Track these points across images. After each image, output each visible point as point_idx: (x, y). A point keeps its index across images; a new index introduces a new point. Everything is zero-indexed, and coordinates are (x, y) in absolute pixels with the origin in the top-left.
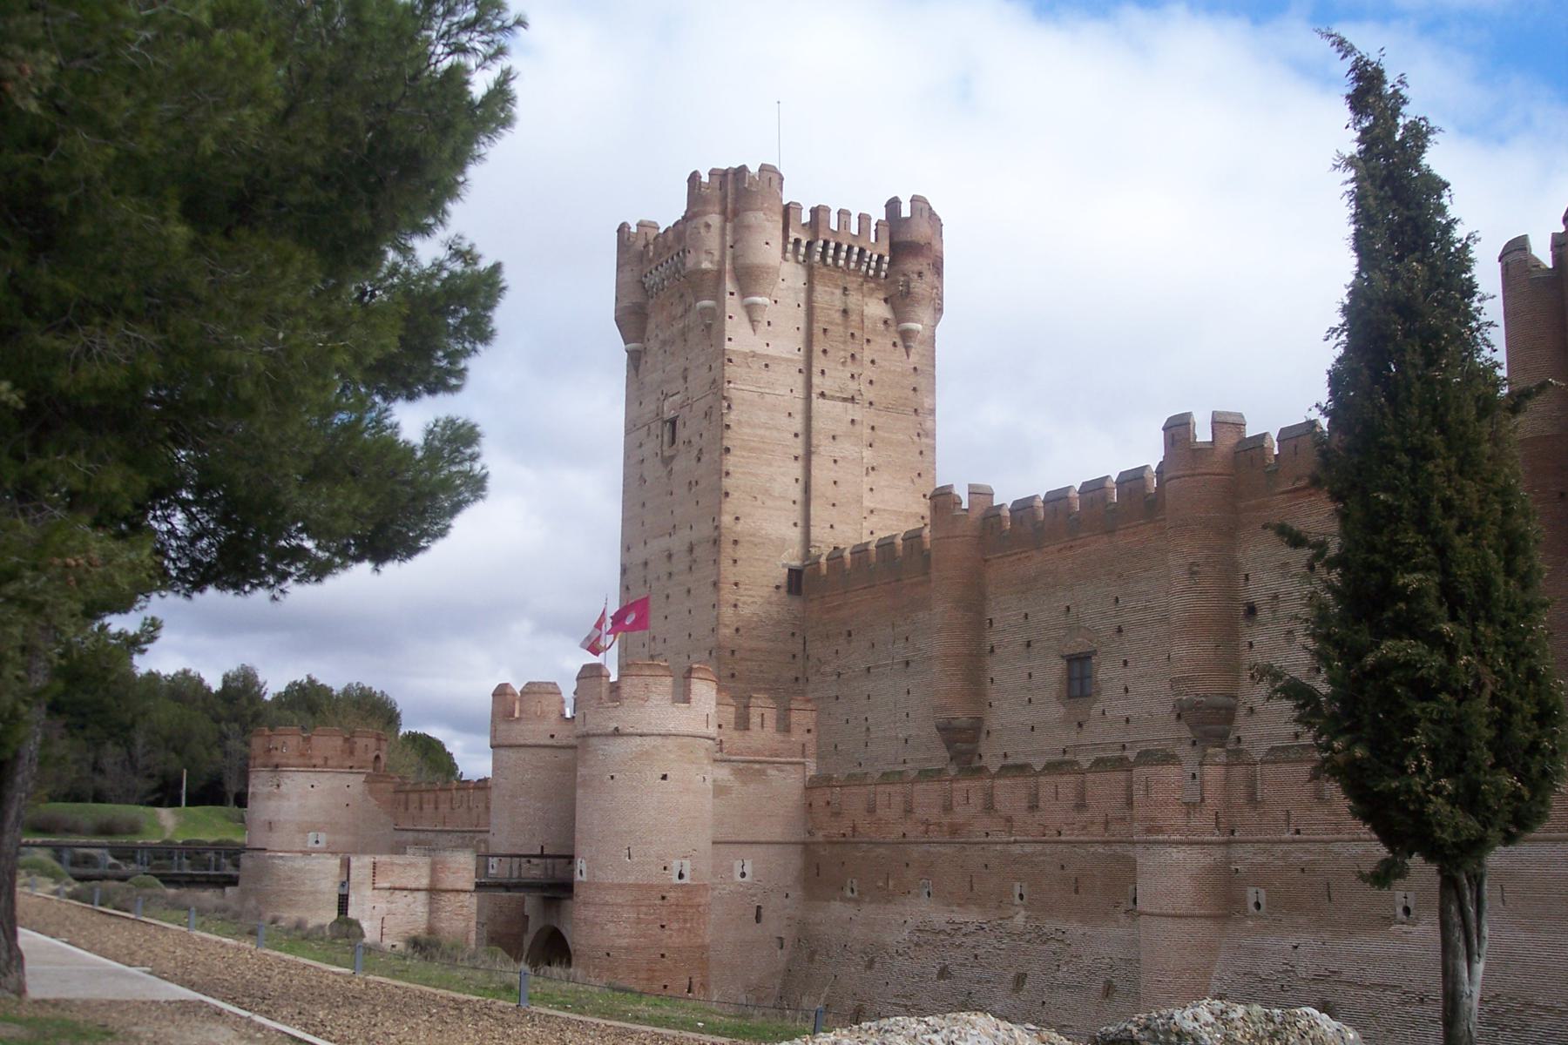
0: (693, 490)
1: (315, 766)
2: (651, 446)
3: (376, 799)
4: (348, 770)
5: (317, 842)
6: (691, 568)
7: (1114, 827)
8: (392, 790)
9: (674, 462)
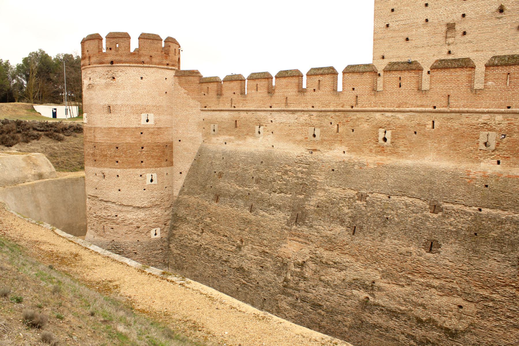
1: (143, 62)
3: (185, 88)
4: (166, 67)
5: (147, 121)
8: (198, 82)
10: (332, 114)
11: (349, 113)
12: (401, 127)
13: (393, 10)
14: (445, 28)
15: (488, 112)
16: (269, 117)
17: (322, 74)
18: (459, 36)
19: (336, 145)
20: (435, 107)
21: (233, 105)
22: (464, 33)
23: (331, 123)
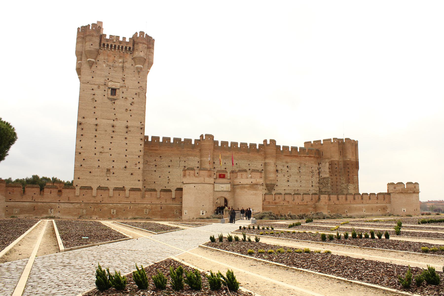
2: (99, 93)
6: (127, 132)
7: (308, 203)
8: (5, 186)
9: (116, 101)
10: (92, 204)
11: (99, 204)
12: (120, 208)
13: (84, 159)
14: (106, 170)
15: (146, 204)
16: (57, 205)
17: (87, 189)
18: (111, 174)
19: (93, 215)
20: (131, 202)
21: (34, 199)
22: (113, 173)
23: (91, 208)
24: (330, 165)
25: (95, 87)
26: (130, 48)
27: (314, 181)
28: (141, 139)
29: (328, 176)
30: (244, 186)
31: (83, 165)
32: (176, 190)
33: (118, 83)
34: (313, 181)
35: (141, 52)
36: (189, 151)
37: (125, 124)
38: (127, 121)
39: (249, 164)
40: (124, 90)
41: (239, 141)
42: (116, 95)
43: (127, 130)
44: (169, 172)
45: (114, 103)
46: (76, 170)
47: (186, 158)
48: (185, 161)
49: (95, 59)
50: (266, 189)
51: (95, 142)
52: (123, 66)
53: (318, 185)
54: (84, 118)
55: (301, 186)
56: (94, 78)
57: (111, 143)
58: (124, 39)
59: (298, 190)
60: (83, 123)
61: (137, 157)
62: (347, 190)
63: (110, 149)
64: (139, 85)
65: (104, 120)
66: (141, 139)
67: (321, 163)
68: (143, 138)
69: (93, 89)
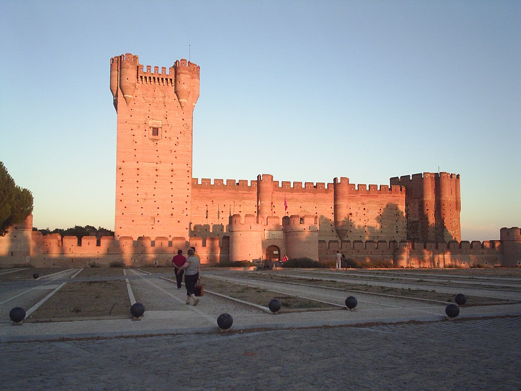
0: (172, 153)
2: (139, 133)
9: (159, 141)
13: (125, 207)
14: (150, 218)
22: (158, 221)
24: (420, 205)
25: (136, 126)
26: (171, 80)
27: (399, 226)
28: (188, 183)
29: (417, 219)
30: (296, 233)
31: (124, 213)
32: (223, 239)
33: (159, 121)
34: (398, 226)
35: (184, 84)
36: (244, 193)
37: (169, 166)
38: (172, 164)
39: (316, 207)
40: (167, 128)
41: (303, 180)
42: (159, 135)
43: (172, 173)
44: (223, 218)
45: (157, 144)
46: (117, 219)
47: (241, 202)
48: (240, 206)
49: (132, 95)
50: (336, 236)
51: (138, 188)
52: (165, 101)
53: (405, 230)
54: (124, 162)
55: (382, 232)
56: (132, 117)
57: (155, 188)
58: (164, 69)
59: (378, 237)
60: (123, 167)
61: (185, 202)
62: (442, 237)
63: (154, 195)
64: (184, 122)
65: (146, 163)
66: (188, 183)
67: (409, 204)
68: (190, 182)
69: (132, 129)
